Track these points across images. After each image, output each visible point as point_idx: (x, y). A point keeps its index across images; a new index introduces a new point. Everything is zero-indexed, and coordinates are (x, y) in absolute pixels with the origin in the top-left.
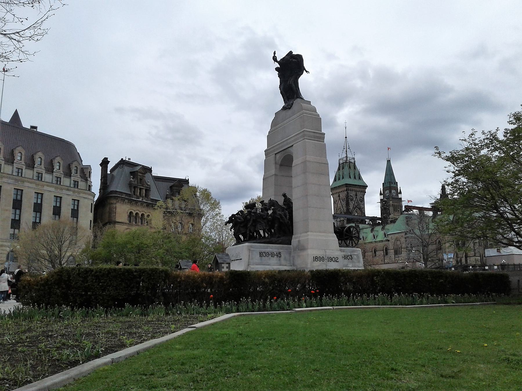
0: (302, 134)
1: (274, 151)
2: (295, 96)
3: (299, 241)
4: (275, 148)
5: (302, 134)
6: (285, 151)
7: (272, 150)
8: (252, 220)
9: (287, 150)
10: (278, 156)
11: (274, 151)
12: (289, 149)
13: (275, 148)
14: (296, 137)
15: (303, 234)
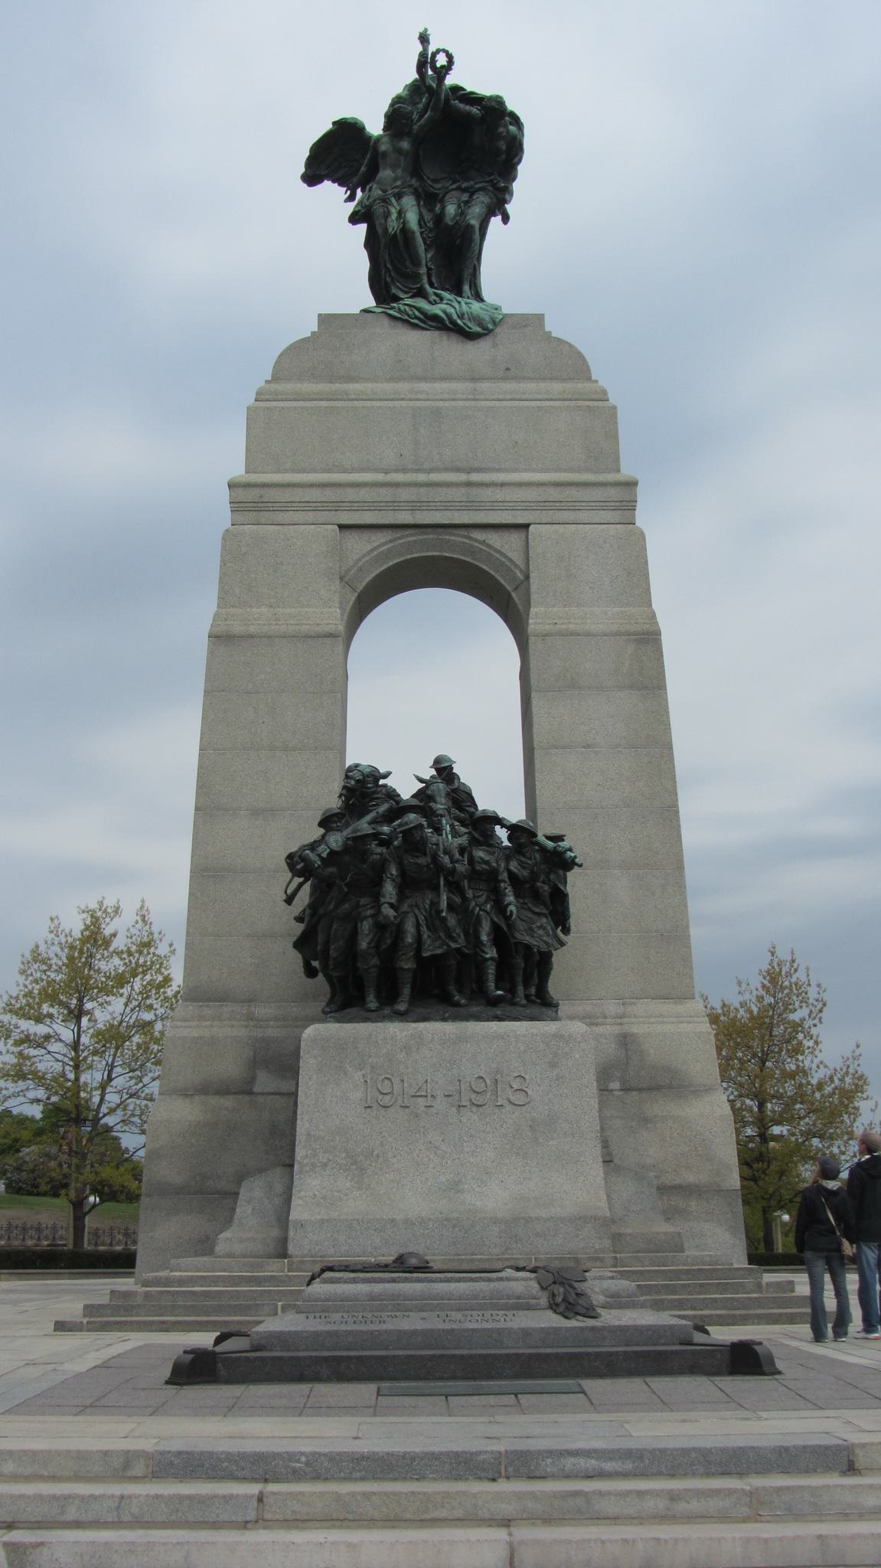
0: (613, 493)
1: (337, 506)
2: (466, 288)
3: (625, 1041)
4: (350, 494)
5: (613, 493)
6: (430, 536)
7: (314, 495)
8: (505, 876)
9: (453, 537)
10: (360, 546)
11: (337, 506)
12: (478, 535)
13: (350, 494)
14: (554, 494)
15: (642, 1007)
